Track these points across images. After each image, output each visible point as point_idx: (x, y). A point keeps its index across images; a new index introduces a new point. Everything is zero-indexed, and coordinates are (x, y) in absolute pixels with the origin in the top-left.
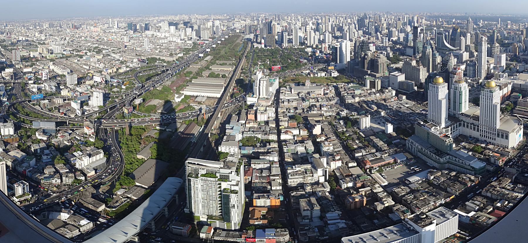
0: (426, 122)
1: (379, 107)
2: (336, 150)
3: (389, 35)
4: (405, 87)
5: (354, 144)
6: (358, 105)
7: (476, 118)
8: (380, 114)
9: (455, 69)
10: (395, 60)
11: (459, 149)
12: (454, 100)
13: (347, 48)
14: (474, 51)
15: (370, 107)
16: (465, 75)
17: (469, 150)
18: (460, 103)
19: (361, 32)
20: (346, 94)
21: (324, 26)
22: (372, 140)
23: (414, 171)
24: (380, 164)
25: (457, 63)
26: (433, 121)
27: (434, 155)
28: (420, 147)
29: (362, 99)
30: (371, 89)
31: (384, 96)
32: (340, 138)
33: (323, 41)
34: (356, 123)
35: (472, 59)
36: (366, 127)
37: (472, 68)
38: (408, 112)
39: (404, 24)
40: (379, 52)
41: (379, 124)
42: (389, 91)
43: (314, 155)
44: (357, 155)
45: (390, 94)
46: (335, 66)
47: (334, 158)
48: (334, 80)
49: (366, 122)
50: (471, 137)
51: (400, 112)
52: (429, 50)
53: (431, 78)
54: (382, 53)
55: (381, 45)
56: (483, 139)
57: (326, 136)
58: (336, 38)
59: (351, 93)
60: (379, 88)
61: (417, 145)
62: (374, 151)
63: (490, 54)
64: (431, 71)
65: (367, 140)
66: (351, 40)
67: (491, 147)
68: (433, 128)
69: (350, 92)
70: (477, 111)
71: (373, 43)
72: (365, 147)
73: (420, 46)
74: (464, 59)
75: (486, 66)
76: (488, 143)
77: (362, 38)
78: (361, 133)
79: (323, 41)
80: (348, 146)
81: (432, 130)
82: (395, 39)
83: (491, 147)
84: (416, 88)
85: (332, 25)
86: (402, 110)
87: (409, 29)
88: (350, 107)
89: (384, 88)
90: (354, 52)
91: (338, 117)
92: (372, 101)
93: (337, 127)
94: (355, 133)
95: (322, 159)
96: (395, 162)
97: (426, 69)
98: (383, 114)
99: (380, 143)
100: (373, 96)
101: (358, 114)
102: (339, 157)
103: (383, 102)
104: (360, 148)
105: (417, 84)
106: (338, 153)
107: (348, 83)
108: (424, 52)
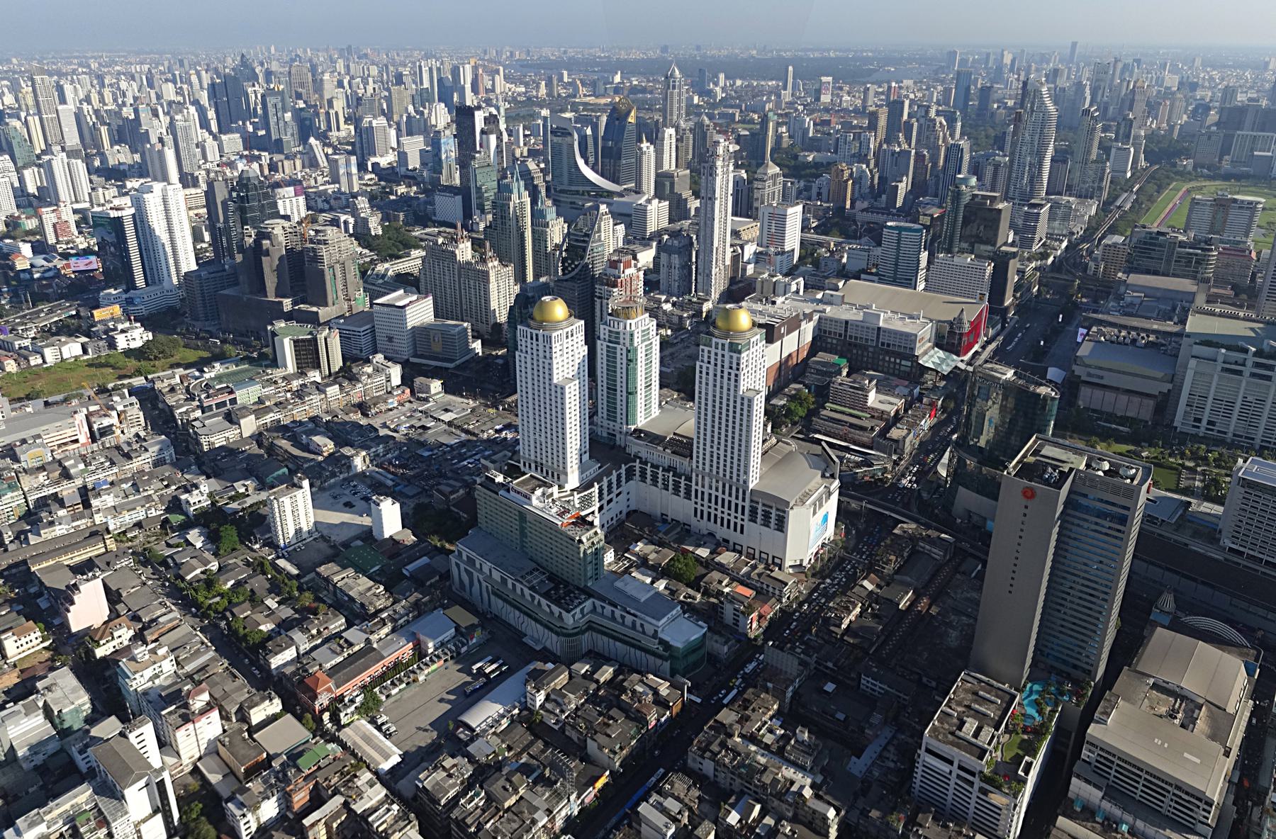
0: (513, 472)
1: (340, 441)
2: (189, 668)
3: (363, 146)
4: (437, 348)
5: (259, 617)
6: (254, 449)
7: (683, 447)
8: (350, 467)
9: (614, 264)
10: (394, 246)
11: (627, 571)
12: (606, 378)
13: (174, 220)
14: (687, 194)
15: (306, 448)
16: (651, 285)
17: (659, 572)
18: (631, 393)
19: (233, 142)
20: (198, 413)
21: (34, 122)
22: (327, 580)
23: (482, 680)
24: (365, 677)
25: (627, 241)
26: (539, 466)
27: (544, 602)
28: (496, 576)
29: (269, 418)
30: (301, 373)
31: (356, 393)
32: (199, 607)
33: (47, 196)
34: (256, 524)
35: (677, 226)
36: (298, 531)
37: (676, 260)
38: (454, 441)
39: (423, 98)
40: (323, 217)
41: (349, 506)
42: (377, 370)
43: (95, 732)
44: (276, 662)
45: (381, 379)
46: (130, 301)
47: (186, 706)
48: (133, 363)
49: (296, 511)
50: (665, 521)
51: (422, 444)
52: (520, 199)
53: (526, 306)
54: (335, 223)
55: (331, 188)
56: (704, 526)
57: (136, 618)
58: (116, 175)
59: (219, 405)
60: (337, 363)
61: (487, 566)
62: (338, 623)
63: (744, 204)
64: (530, 278)
65: (308, 587)
66: (188, 180)
67: (727, 558)
68: (539, 492)
69: (212, 402)
70: (685, 422)
71: (293, 182)
72: (300, 621)
73: (488, 183)
74: (652, 227)
75: (729, 250)
76: (718, 544)
77: (241, 166)
78: (282, 563)
79: (47, 196)
80: (236, 632)
81: (535, 502)
82: (386, 160)
83: (727, 558)
84: (477, 346)
85: (79, 117)
86: (430, 437)
87: (440, 116)
88: (221, 464)
89: (354, 358)
90: (212, 229)
91: (176, 519)
92: (314, 419)
93: (178, 566)
94: (259, 567)
95: (132, 737)
96: (419, 653)
97: (510, 269)
98: (360, 462)
99: (358, 586)
100: (316, 398)
101: (263, 486)
102: (205, 697)
103: (356, 417)
104: (285, 626)
105: (483, 328)
106: (197, 679)
107: (201, 365)
108: (501, 207)
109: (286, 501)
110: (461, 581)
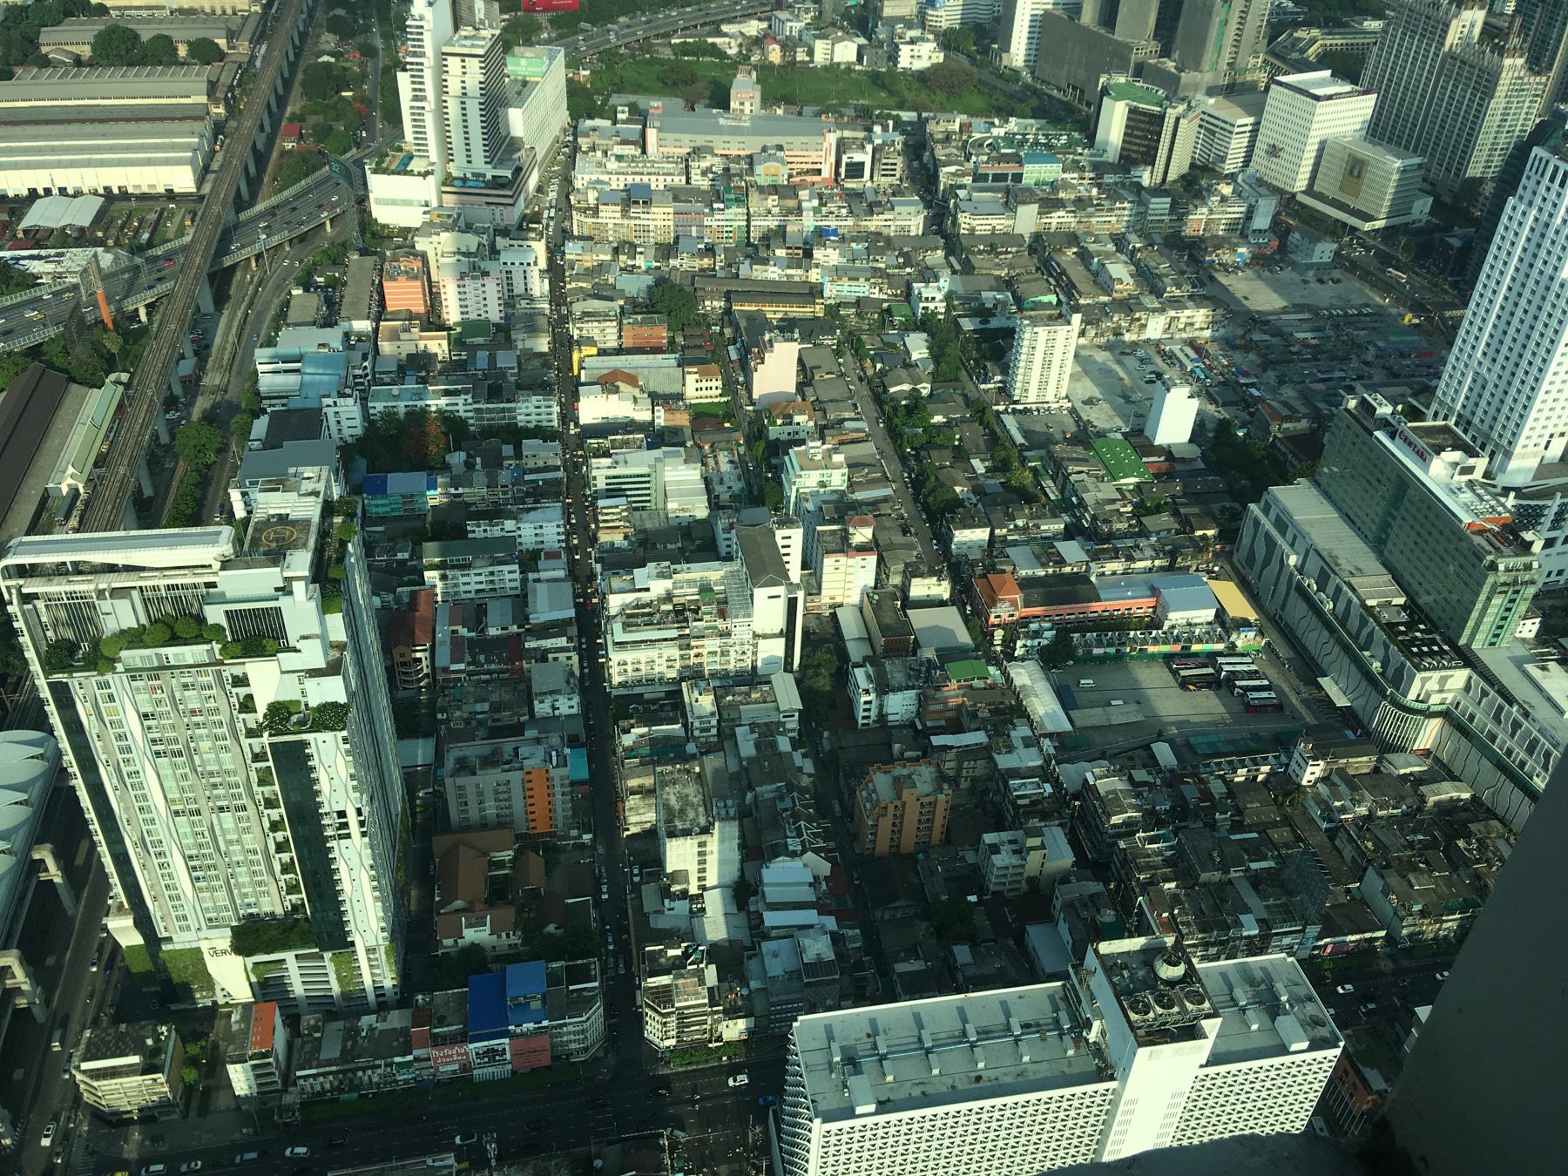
109: (1042, 332)
110: (1252, 552)
